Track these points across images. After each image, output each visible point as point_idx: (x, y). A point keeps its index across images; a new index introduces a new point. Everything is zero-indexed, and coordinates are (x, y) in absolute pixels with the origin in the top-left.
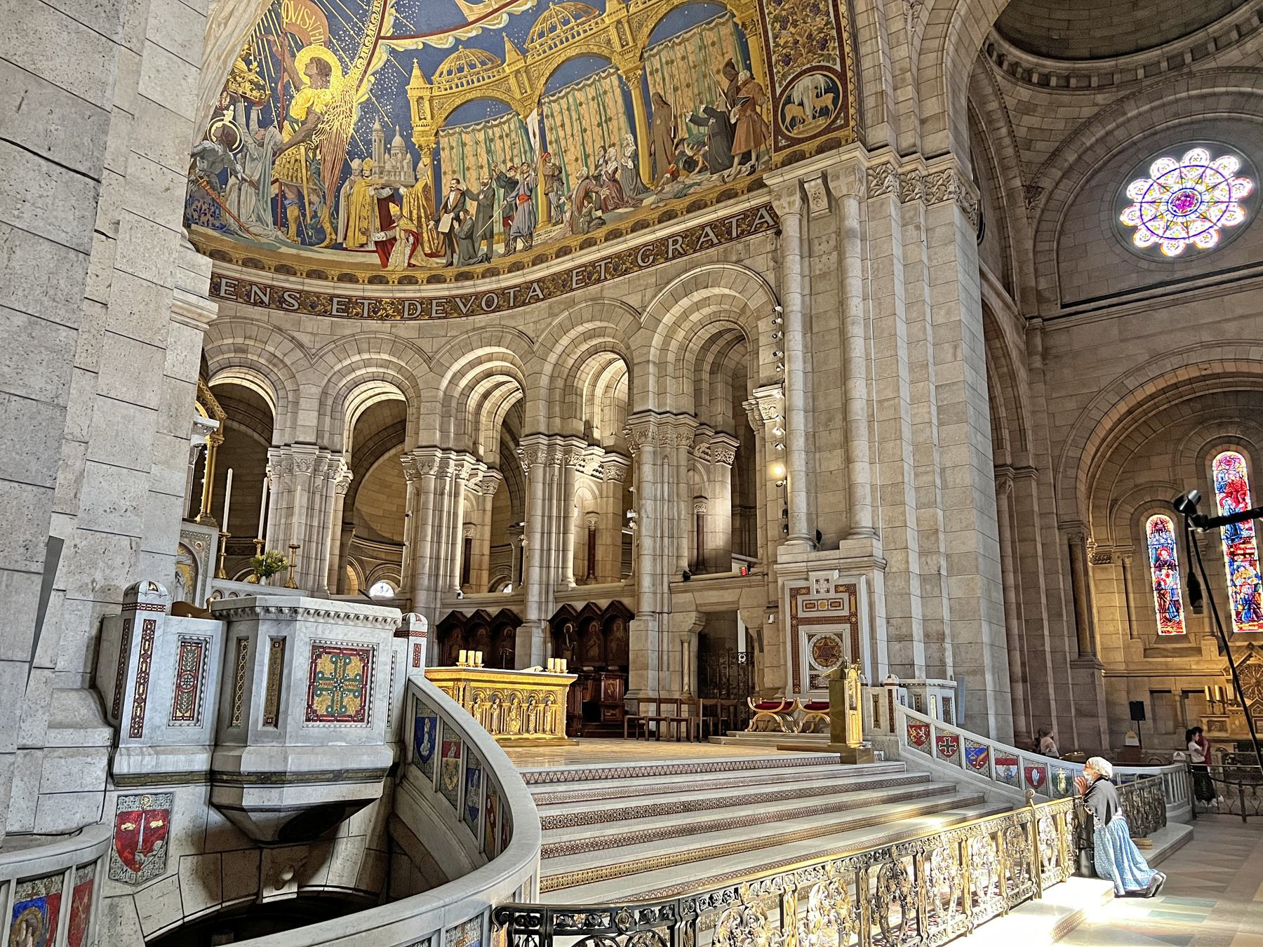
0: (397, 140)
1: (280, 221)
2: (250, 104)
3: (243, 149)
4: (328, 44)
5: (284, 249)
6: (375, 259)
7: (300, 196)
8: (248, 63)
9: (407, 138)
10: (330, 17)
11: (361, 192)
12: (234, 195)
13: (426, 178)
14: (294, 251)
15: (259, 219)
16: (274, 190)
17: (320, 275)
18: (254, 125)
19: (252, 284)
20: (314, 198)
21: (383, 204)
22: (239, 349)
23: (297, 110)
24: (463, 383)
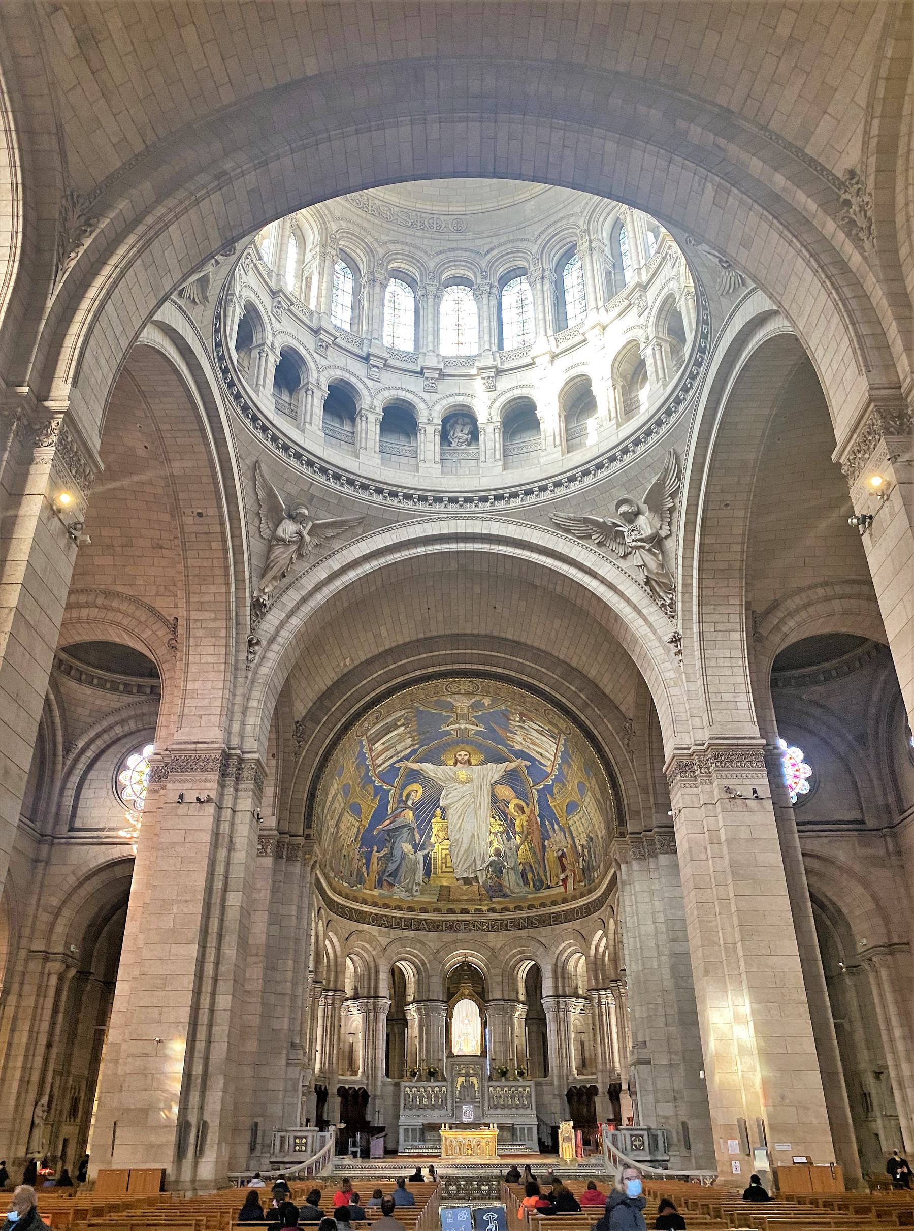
0: (556, 826)
1: (526, 883)
2: (502, 833)
3: (505, 854)
4: (518, 797)
5: (530, 896)
6: (562, 889)
7: (531, 866)
8: (494, 818)
9: (558, 824)
10: (512, 787)
11: (552, 855)
12: (506, 878)
13: (569, 840)
14: (533, 896)
15: (518, 885)
16: (521, 867)
17: (543, 905)
18: (506, 842)
19: (519, 918)
20: (537, 866)
21: (560, 858)
22: (521, 952)
23: (518, 829)
24: (601, 949)
